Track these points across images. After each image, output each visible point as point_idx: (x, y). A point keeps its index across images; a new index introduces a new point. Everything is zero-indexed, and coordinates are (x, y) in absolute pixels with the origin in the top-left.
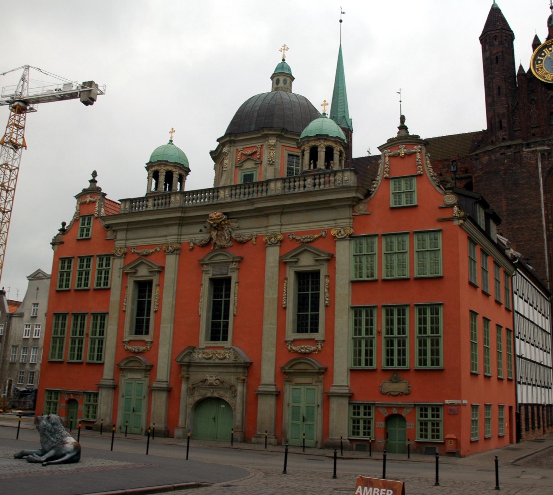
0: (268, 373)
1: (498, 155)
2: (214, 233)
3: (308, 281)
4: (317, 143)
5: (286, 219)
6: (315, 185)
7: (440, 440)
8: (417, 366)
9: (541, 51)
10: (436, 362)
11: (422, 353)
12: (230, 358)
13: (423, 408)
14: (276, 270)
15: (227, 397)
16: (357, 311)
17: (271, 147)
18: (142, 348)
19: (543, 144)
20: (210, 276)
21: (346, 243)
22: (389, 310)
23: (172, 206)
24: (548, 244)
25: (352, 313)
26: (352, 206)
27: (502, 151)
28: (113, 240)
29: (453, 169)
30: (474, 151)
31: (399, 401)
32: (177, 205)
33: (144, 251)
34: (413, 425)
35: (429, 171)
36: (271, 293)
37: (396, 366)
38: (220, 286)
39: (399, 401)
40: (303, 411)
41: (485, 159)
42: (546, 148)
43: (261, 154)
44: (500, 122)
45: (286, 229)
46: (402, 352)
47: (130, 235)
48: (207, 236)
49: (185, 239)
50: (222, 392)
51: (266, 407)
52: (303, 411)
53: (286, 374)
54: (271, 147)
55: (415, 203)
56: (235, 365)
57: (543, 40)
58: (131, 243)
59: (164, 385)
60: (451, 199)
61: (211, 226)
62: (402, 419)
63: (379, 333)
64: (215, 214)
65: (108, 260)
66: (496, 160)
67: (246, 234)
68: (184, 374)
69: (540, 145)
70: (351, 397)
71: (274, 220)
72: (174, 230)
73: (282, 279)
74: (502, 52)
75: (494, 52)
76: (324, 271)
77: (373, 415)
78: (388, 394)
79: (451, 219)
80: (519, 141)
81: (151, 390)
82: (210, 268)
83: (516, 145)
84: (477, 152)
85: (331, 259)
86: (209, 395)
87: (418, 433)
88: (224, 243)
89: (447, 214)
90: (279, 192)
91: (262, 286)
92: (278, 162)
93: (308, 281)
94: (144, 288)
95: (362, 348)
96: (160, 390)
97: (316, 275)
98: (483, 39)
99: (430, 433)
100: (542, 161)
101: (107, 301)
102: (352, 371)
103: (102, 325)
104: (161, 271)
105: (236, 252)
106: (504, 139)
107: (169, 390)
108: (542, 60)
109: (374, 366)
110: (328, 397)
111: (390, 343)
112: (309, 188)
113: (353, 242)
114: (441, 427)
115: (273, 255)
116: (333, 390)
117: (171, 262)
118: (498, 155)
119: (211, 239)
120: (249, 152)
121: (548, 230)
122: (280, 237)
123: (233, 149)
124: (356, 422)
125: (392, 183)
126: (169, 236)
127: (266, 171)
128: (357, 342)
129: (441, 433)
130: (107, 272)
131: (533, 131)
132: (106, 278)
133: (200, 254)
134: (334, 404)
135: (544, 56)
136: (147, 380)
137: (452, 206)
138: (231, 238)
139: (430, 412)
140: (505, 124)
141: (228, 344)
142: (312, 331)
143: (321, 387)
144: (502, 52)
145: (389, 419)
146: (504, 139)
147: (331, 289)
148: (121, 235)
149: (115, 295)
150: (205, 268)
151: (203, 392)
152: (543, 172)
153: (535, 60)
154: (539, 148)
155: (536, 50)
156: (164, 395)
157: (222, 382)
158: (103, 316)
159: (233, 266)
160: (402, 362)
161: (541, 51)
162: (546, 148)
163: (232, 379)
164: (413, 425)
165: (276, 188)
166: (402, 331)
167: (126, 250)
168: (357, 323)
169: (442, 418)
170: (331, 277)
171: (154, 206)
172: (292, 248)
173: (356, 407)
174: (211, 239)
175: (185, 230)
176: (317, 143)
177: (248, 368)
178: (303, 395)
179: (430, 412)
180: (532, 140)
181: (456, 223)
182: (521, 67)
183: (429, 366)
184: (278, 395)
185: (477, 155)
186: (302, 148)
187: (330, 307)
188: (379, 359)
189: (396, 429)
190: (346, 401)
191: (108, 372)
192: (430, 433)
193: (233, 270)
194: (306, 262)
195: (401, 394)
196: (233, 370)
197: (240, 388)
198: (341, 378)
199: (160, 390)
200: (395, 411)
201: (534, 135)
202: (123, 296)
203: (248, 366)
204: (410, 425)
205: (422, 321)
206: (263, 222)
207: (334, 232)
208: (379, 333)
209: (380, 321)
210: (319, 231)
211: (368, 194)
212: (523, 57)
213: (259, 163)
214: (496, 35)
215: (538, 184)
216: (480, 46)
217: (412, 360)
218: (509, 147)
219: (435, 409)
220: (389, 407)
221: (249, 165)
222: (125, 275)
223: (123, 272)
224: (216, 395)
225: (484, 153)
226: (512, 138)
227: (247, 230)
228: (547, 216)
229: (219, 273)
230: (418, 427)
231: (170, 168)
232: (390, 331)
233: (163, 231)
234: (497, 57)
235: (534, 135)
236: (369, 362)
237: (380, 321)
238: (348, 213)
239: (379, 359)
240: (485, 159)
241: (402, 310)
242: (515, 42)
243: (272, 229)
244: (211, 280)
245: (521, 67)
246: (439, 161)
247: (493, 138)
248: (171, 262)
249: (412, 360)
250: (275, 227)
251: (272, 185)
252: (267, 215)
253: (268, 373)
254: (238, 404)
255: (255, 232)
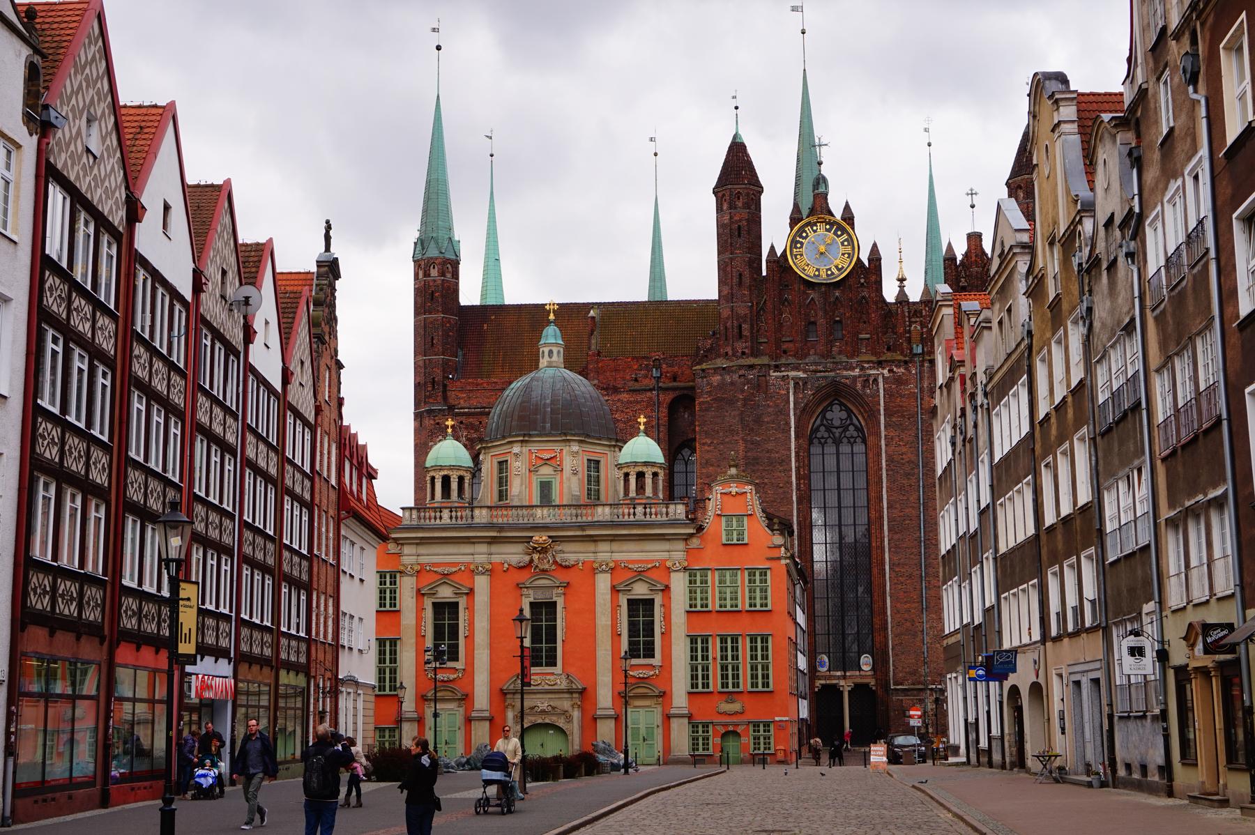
0: (605, 697)
1: (735, 377)
2: (536, 556)
3: (641, 609)
4: (644, 469)
5: (615, 546)
6: (645, 514)
7: (772, 751)
8: (750, 689)
9: (802, 230)
10: (766, 685)
11: (754, 677)
12: (563, 684)
13: (756, 725)
14: (609, 596)
15: (561, 723)
16: (693, 640)
17: (575, 454)
18: (452, 677)
19: (797, 368)
20: (532, 600)
21: (681, 575)
22: (723, 640)
23: (476, 520)
24: (798, 509)
25: (688, 640)
26: (686, 540)
27: (741, 372)
28: (399, 555)
29: (655, 373)
30: (698, 364)
31: (735, 720)
32: (484, 521)
33: (446, 570)
34: (747, 740)
35: (759, 513)
36: (603, 620)
37: (730, 689)
38: (544, 609)
39: (735, 720)
40: (643, 732)
41: (716, 379)
42: (801, 374)
43: (561, 461)
44: (740, 327)
45: (617, 556)
46: (736, 677)
47: (423, 550)
48: (527, 558)
49: (496, 559)
50: (554, 718)
51: (606, 731)
52: (643, 732)
53: (624, 698)
54: (575, 454)
55: (746, 541)
56: (570, 692)
57: (805, 212)
58: (423, 560)
59: (487, 714)
60: (778, 540)
61: (535, 548)
62: (735, 733)
63: (715, 659)
64: (540, 538)
65: (393, 577)
66: (732, 383)
67: (571, 558)
68: (509, 701)
69: (793, 370)
70: (690, 717)
71: (603, 546)
72: (483, 548)
73: (615, 607)
74: (748, 220)
75: (736, 218)
76: (658, 600)
77: (711, 733)
78: (725, 713)
79: (779, 559)
80: (765, 360)
81: (468, 721)
82: (531, 592)
83: (762, 366)
84: (704, 366)
85: (666, 589)
86: (540, 721)
87: (752, 746)
88: (547, 567)
89: (775, 554)
90: (608, 518)
91: (593, 612)
92: (580, 469)
93: (641, 609)
94: (446, 614)
95: (698, 675)
96: (483, 719)
97: (650, 603)
98: (720, 190)
99: (762, 746)
100: (795, 393)
101: (398, 625)
102: (689, 693)
103: (394, 652)
104: (471, 593)
105: (562, 577)
106: (743, 353)
107: (491, 720)
108: (802, 244)
109: (711, 689)
110: (667, 718)
111: (724, 668)
112: (640, 516)
113: (687, 574)
114: (772, 741)
115: (603, 583)
116: (673, 711)
117: (482, 584)
118: (735, 377)
119: (532, 561)
120: (548, 456)
121: (798, 489)
122: (612, 565)
123: (525, 450)
124: (695, 739)
125: (723, 519)
126: (480, 555)
127: (569, 479)
128: (694, 669)
129: (772, 745)
130: (393, 592)
131: (784, 347)
132: (393, 598)
133: (523, 577)
134: (675, 724)
135: (805, 238)
136: (462, 710)
137: (780, 546)
138: (555, 562)
139: (762, 728)
140: (746, 333)
141: (558, 669)
142: (645, 657)
143: (660, 709)
144: (748, 220)
145: (725, 735)
146: (743, 353)
147: (667, 618)
148: (407, 550)
149: (408, 618)
150: (525, 591)
151: (533, 719)
152: (795, 409)
153: (794, 243)
154: (792, 374)
155: (796, 228)
156: (487, 724)
157: (553, 708)
158: (394, 642)
159: (560, 591)
160: (736, 685)
161: (802, 230)
162: (801, 374)
163: (566, 705)
164: (747, 740)
165: (603, 513)
166: (735, 657)
167: (419, 568)
168: (693, 650)
169: (772, 732)
170: (667, 606)
171: (451, 518)
172: (623, 575)
173: (694, 727)
174: (532, 561)
175: (494, 548)
176: (644, 469)
177: (584, 695)
178: (643, 717)
179: (762, 728)
180: (783, 361)
181: (783, 562)
182: (772, 248)
183: (760, 688)
184: (619, 720)
185: (703, 370)
186: (625, 470)
187: (666, 634)
188: (715, 683)
189: (732, 746)
190: (686, 720)
191: (409, 706)
192: (762, 746)
193: (558, 595)
194: (640, 591)
195: (736, 713)
196: (566, 696)
197: (576, 714)
198: (680, 699)
199: (483, 719)
200: (731, 728)
201: (785, 352)
202: (419, 619)
203: (583, 692)
204: (744, 740)
205: (754, 649)
206: (590, 547)
207: (669, 564)
208: (715, 659)
209: (715, 648)
210: (652, 561)
211: (700, 529)
212: (775, 232)
213: (559, 469)
214: (738, 182)
215: (788, 424)
216: (714, 198)
217: (745, 683)
218: (751, 367)
219: (767, 725)
220: (725, 725)
221: (546, 470)
222: (420, 594)
223: (418, 591)
224: (547, 721)
225: (715, 369)
226: (755, 354)
227: (572, 554)
228: (798, 469)
229: (541, 597)
230: (752, 741)
231: (461, 473)
232: (724, 657)
233: (467, 549)
234: (739, 227)
235: (785, 352)
236: (706, 685)
237: (715, 648)
238: (681, 545)
239: (715, 683)
240: (716, 379)
241: (735, 639)
242: (762, 197)
243: (603, 556)
244: (531, 603)
245: (772, 248)
246: (633, 358)
247: (729, 350)
248: (482, 584)
249: (745, 683)
250: (605, 553)
251: (600, 509)
252: (595, 541)
253: (605, 697)
254: (575, 728)
255: (582, 557)
